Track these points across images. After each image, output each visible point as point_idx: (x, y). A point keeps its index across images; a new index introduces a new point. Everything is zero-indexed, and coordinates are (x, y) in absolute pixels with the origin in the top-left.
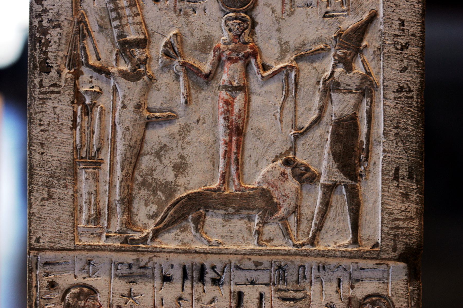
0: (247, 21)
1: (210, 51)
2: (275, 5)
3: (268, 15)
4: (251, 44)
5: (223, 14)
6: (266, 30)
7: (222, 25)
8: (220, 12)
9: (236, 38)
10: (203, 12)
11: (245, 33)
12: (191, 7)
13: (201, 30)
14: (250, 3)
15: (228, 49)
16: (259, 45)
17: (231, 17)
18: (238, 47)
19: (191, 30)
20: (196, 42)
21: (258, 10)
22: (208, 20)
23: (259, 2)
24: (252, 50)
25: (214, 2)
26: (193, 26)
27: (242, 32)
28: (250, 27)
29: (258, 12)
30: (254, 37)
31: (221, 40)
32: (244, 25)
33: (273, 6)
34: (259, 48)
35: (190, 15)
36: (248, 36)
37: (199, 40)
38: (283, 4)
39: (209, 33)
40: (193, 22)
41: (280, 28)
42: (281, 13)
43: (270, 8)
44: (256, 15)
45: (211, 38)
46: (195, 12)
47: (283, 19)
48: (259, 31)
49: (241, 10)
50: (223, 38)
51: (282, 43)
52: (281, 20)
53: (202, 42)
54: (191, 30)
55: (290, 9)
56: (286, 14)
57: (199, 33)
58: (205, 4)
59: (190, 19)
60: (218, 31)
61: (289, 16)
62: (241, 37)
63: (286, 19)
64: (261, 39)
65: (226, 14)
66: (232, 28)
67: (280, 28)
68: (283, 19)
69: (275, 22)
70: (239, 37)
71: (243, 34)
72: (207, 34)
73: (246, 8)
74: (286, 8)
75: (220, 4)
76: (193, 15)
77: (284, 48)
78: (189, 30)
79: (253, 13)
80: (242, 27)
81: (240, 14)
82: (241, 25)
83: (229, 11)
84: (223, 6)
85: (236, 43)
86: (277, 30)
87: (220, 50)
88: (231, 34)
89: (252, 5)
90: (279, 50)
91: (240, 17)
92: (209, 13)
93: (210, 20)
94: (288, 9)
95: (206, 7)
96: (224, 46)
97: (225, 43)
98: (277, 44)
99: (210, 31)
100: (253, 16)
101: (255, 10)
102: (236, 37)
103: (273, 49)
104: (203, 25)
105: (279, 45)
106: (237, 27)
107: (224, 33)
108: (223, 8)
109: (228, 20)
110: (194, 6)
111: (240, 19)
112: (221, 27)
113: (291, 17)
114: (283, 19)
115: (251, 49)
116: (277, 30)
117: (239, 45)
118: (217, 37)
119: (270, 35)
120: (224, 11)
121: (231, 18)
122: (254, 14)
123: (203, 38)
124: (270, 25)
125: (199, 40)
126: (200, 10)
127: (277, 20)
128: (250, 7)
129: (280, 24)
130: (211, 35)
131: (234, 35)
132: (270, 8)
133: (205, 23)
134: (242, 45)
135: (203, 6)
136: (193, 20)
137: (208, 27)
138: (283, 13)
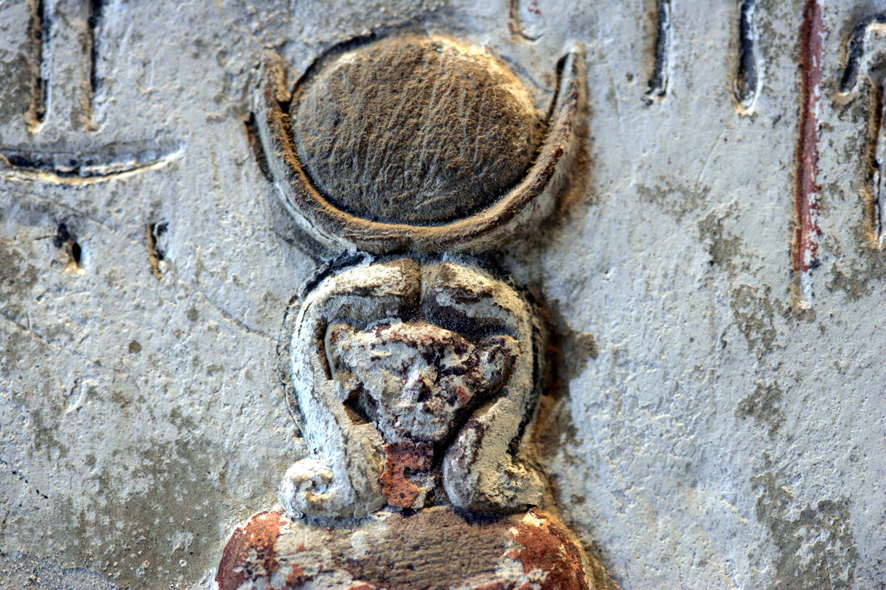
0: (498, 327)
1: (193, 576)
2: (734, 196)
3: (672, 278)
4: (530, 519)
5: (306, 267)
6: (659, 406)
7: (297, 366)
8: (283, 250)
9: (408, 472)
10: (138, 252)
11: (480, 429)
12: (45, 209)
13: (117, 398)
14: (531, 180)
15: (341, 560)
16: (602, 533)
17: (366, 292)
18: (424, 543)
19: (35, 402)
20: (80, 502)
21: (597, 243)
22: (178, 319)
23: (599, 177)
24: (539, 574)
25: (227, 168)
26: (52, 363)
27: (463, 418)
28: (523, 378)
29: (591, 259)
30: (557, 464)
31: (287, 487)
32: (471, 366)
33: (720, 209)
34: (594, 550)
35: (33, 275)
36: (513, 450)
37: (103, 480)
38: (801, 195)
39: (188, 422)
40: (52, 334)
41: (773, 394)
42: (786, 263)
43: (691, 223)
44: (579, 283)
45: (205, 468)
46: (76, 254)
47: (801, 315)
48: (605, 415)
49: (450, 241)
50: (297, 470)
51: (792, 513)
52: (779, 323)
53: (124, 494)
54: (35, 402)
55: (858, 234)
56: (823, 276)
57: (107, 428)
58: (159, 188)
59: (29, 306)
60: (259, 410)
61: (854, 295)
62: (451, 463)
63: (822, 315)
64: (619, 480)
65: (329, 272)
66: (374, 388)
67: (773, 394)
68: (794, 315)
69: (734, 337)
70: (436, 464)
71: (467, 437)
72: (169, 433)
73: (492, 226)
74: (823, 223)
75: (283, 188)
76: (54, 276)
77: (804, 555)
78: (19, 401)
79: (550, 262)
80: (457, 381)
81: (447, 276)
82: (452, 361)
83: (352, 250)
84: (306, 204)
85: (408, 512)
86: (748, 409)
87: (271, 567)
88: (363, 433)
89: (545, 201)
90: (766, 569)
91: (444, 300)
92: (190, 262)
93: (193, 315)
94: (845, 238)
95: (166, 214)
96: (308, 536)
97: (316, 507)
98: (752, 521)
99: (198, 412)
100: (555, 291)
101: (565, 236)
102: (407, 461)
103: (718, 564)
104: (142, 359)
105: (763, 531)
106: (414, 376)
107: (311, 427)
108: (301, 220)
109: (343, 316)
110: (69, 198)
111: (442, 317)
112: (284, 375)
113: (863, 304)
114: (794, 315)
115: (528, 559)
116: (748, 409)
117: (434, 532)
118: (249, 457)
119: (694, 448)
120: (314, 248)
121: (369, 306)
122: (562, 276)
123: (134, 463)
124: (691, 361)
125: (103, 480)
126: (120, 236)
127: (748, 326)
128: (525, 215)
129: (773, 360)
130: (204, 443)
131: (393, 448)
132: (691, 223)
133: (154, 342)
134: (458, 524)
135: (144, 201)
136: (53, 319)
137: (182, 380)
138: (798, 266)
